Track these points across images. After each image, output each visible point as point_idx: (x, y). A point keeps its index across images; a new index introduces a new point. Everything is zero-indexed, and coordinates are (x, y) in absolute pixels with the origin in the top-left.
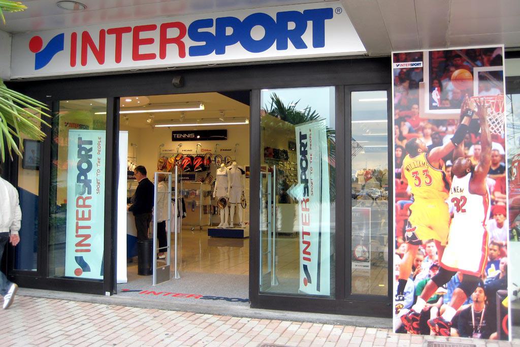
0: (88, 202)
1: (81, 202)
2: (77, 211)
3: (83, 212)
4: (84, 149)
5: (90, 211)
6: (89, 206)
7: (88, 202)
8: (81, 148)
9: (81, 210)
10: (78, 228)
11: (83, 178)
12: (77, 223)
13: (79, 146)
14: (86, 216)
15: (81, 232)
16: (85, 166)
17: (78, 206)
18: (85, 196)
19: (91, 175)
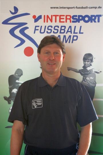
0: (68, 21)
2: (64, 16)
3: (63, 19)
4: (95, 18)
5: (64, 22)
6: (66, 22)
7: (68, 21)
8: (95, 16)
9: (65, 17)
10: (56, 16)
11: (81, 18)
12: (58, 16)
13: (97, 16)
14: (62, 20)
15: (54, 18)
16: (87, 19)
17: (66, 16)
19: (82, 22)
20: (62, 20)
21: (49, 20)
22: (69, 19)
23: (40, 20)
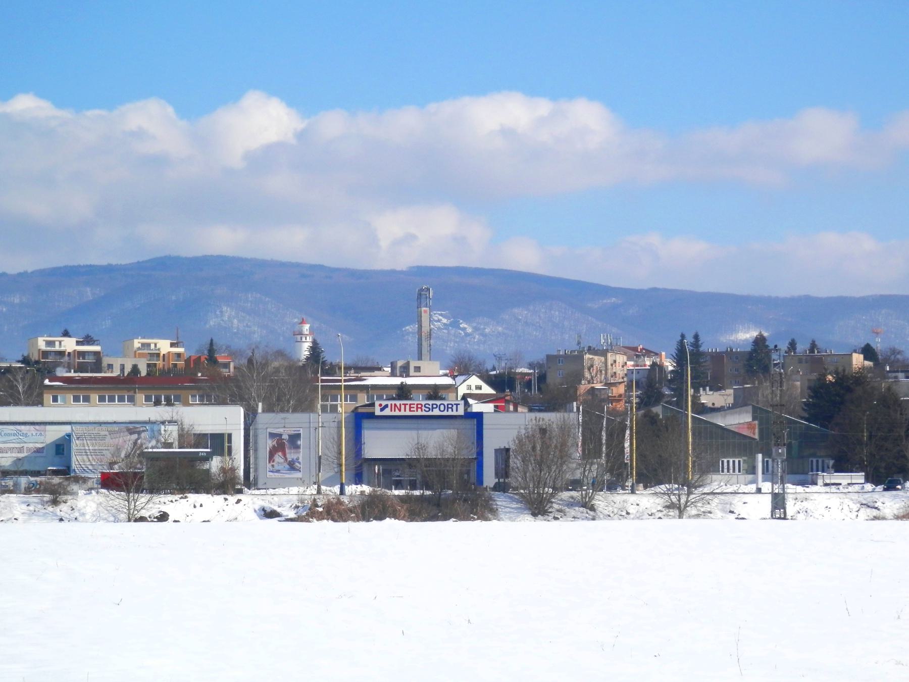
0: (419, 410)
2: (414, 404)
3: (414, 408)
5: (414, 411)
6: (417, 411)
7: (419, 410)
9: (415, 406)
10: (405, 405)
12: (407, 404)
14: (412, 409)
15: (403, 407)
16: (442, 408)
17: (417, 404)
18: (423, 408)
20: (412, 409)
21: (396, 409)
22: (421, 408)
23: (387, 409)
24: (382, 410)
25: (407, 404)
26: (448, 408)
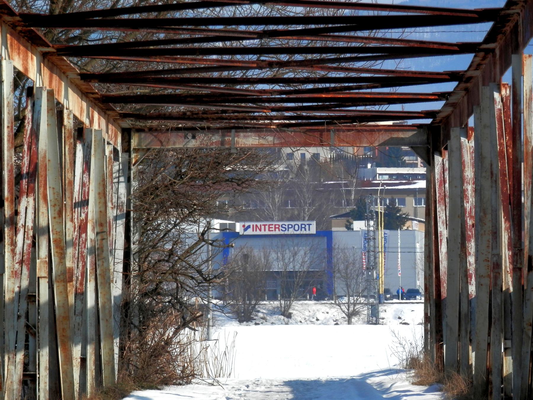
0: (277, 230)
1: (303, 226)
2: (272, 225)
3: (272, 228)
5: (273, 231)
6: (275, 230)
7: (277, 230)
9: (273, 226)
12: (267, 225)
14: (271, 229)
15: (263, 227)
16: (296, 227)
17: (275, 225)
18: (280, 228)
20: (271, 229)
21: (257, 229)
22: (278, 228)
24: (246, 230)
25: (267, 225)
26: (302, 228)
